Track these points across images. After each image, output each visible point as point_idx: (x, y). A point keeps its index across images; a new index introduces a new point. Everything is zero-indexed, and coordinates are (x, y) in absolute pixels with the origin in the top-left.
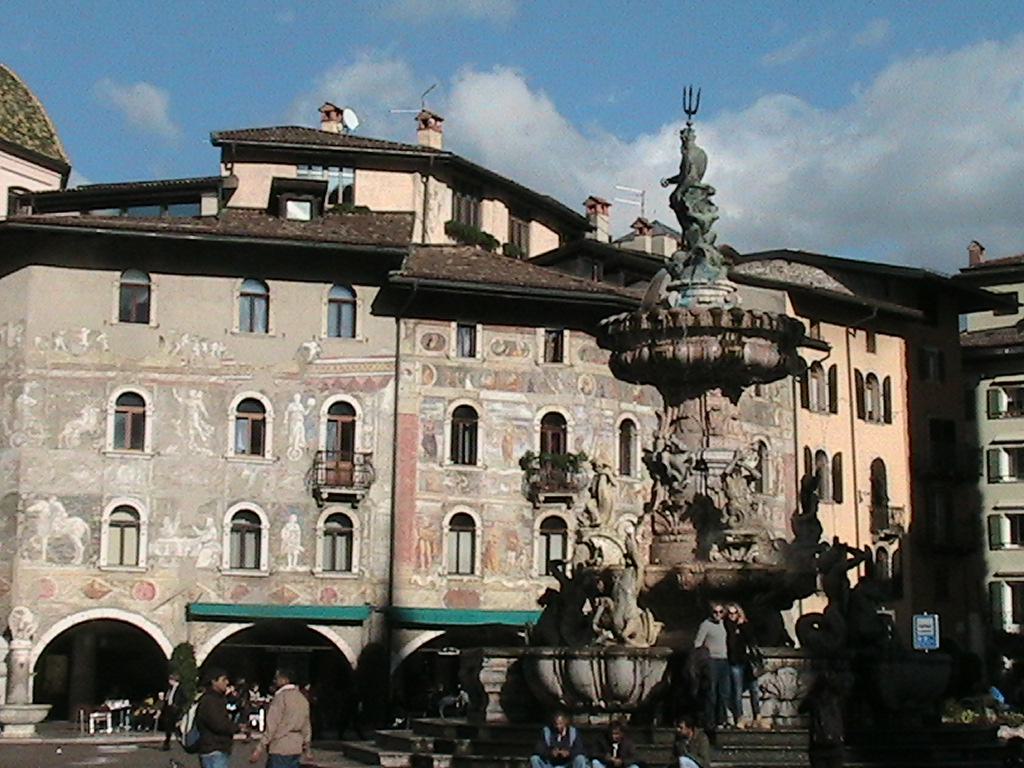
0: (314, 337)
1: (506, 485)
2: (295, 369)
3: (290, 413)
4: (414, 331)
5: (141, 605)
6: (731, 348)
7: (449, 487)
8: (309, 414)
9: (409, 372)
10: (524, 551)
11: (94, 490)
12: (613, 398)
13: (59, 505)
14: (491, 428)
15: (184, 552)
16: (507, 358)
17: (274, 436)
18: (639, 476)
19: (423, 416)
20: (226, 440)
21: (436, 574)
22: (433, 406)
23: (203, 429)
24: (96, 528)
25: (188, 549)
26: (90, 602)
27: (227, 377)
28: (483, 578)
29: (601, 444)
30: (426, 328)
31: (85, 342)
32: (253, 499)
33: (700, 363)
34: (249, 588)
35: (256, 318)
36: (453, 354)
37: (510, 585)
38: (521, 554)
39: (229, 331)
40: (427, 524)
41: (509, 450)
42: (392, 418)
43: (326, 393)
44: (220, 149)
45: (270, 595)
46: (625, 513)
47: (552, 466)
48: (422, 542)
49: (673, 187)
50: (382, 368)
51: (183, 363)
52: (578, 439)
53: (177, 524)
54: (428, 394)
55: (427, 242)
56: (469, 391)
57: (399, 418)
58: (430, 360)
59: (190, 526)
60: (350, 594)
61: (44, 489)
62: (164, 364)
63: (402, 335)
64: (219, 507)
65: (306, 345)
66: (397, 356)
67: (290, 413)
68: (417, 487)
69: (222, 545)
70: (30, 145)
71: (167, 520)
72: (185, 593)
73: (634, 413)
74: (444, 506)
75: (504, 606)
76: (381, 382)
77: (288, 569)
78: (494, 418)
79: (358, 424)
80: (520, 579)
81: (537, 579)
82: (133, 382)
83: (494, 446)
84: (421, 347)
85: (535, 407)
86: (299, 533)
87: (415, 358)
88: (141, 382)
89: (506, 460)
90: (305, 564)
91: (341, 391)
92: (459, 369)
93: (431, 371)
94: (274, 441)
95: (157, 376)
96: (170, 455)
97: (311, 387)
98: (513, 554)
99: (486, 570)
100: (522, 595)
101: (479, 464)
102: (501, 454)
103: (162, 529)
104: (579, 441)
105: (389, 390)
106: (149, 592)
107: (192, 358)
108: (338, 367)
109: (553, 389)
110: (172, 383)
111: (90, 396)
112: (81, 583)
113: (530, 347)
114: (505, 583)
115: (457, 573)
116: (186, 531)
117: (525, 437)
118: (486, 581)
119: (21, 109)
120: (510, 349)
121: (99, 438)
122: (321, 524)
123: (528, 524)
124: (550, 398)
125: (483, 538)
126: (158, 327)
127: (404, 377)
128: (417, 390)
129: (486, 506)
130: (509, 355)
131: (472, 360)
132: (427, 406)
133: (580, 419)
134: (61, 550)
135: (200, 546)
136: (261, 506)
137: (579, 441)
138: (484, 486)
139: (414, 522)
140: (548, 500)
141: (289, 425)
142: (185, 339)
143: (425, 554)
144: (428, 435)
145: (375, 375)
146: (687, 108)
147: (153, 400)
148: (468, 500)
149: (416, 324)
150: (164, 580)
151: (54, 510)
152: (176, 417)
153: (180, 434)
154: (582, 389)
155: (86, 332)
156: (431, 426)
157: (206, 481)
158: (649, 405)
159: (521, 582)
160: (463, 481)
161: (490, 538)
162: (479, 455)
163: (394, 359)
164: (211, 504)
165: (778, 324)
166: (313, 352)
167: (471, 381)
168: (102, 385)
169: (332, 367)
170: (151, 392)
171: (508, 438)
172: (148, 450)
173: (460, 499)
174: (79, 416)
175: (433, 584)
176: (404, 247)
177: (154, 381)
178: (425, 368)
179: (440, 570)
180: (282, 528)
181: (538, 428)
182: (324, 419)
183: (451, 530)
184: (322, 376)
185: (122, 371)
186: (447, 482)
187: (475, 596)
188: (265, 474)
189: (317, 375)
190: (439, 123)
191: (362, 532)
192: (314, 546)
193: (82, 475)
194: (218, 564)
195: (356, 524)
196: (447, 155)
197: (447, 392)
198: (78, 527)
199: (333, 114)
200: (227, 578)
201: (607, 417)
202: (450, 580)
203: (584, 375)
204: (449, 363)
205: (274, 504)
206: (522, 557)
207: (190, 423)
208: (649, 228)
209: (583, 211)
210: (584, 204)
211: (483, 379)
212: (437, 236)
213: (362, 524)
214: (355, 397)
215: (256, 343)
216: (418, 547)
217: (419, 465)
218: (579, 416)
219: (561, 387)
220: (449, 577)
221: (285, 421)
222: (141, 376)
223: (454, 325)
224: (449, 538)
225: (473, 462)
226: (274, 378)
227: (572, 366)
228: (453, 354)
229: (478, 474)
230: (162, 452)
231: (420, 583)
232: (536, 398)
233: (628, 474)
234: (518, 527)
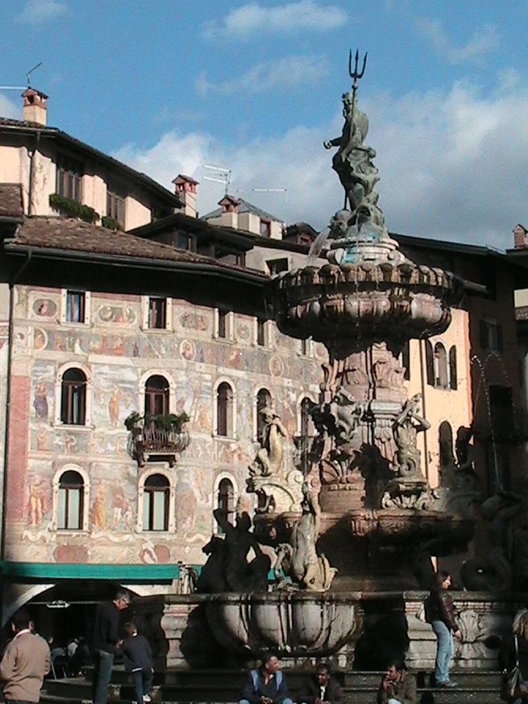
1: (112, 444)
6: (399, 304)
7: (60, 446)
10: (130, 507)
12: (212, 363)
14: (99, 389)
16: (114, 323)
18: (235, 436)
19: (35, 378)
21: (47, 530)
22: (45, 369)
28: (90, 533)
29: (201, 406)
30: (37, 294)
33: (369, 318)
36: (63, 319)
37: (116, 540)
38: (127, 510)
40: (37, 482)
41: (116, 411)
42: (6, 380)
46: (222, 471)
47: (157, 430)
48: (33, 499)
49: (336, 149)
52: (179, 401)
54: (39, 357)
55: (33, 213)
56: (77, 355)
58: (39, 324)
63: (16, 301)
68: (29, 446)
73: (230, 377)
74: (53, 463)
75: (110, 560)
78: (102, 381)
80: (126, 534)
81: (141, 534)
83: (102, 406)
85: (140, 370)
87: (29, 323)
89: (112, 420)
92: (70, 334)
93: (43, 336)
98: (120, 510)
99: (93, 525)
100: (126, 550)
101: (88, 424)
102: (108, 414)
104: (181, 402)
109: (157, 353)
113: (136, 313)
114: (112, 538)
115: (66, 528)
117: (130, 399)
118: (94, 535)
120: (116, 315)
123: (134, 481)
124: (152, 362)
125: (90, 494)
127: (17, 340)
128: (30, 354)
129: (94, 464)
130: (115, 321)
131: (80, 325)
132: (39, 368)
133: (181, 383)
137: (181, 402)
138: (93, 445)
139: (26, 481)
140: (152, 459)
143: (36, 511)
144: (40, 397)
146: (353, 72)
148: (77, 458)
149: (28, 291)
154: (184, 354)
156: (42, 388)
158: (243, 370)
159: (126, 537)
160: (72, 440)
161: (98, 495)
162: (88, 417)
163: (7, 324)
165: (443, 280)
167: (80, 345)
171: (115, 399)
173: (68, 457)
175: (43, 539)
176: (18, 216)
178: (37, 332)
179: (50, 525)
181: (143, 391)
183: (60, 487)
186: (58, 441)
187: (84, 551)
190: (44, 100)
196: (54, 131)
197: (58, 355)
201: (207, 381)
202: (60, 535)
203: (186, 341)
204: (59, 328)
206: (127, 513)
208: (236, 205)
209: (172, 189)
210: (173, 182)
211: (91, 343)
212: (43, 208)
216: (30, 504)
217: (31, 425)
218: (180, 379)
219: (163, 351)
220: (58, 533)
223: (64, 291)
224: (59, 495)
225: (81, 421)
227: (174, 332)
228: (63, 319)
229: (86, 434)
231: (31, 538)
232: (141, 362)
233: (225, 434)
234: (123, 484)
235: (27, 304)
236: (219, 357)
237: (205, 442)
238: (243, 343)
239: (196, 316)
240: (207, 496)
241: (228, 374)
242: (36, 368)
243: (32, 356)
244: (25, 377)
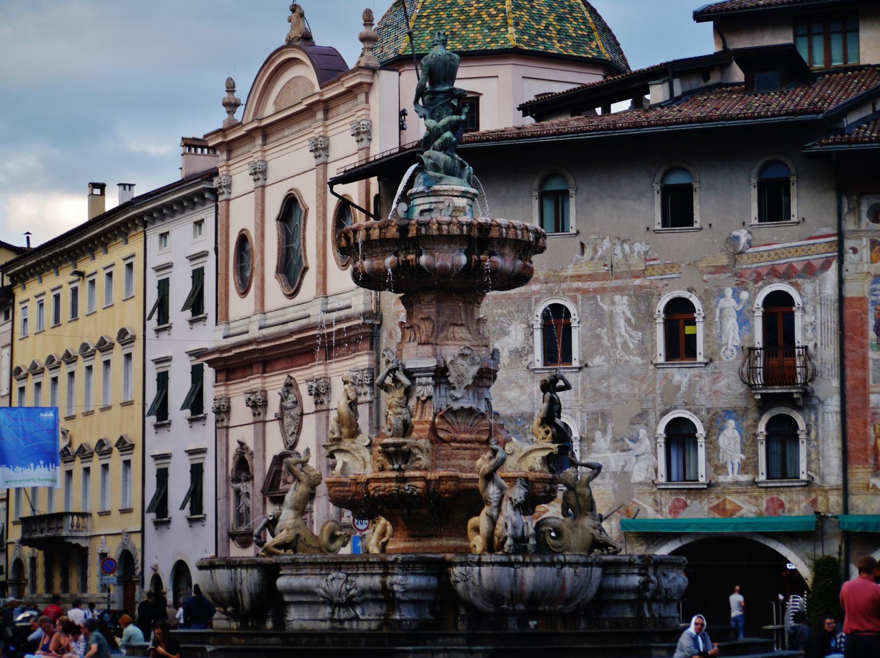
0: (744, 223)
2: (724, 260)
3: (721, 311)
4: (859, 204)
8: (743, 308)
9: (855, 250)
15: (617, 466)
17: (706, 336)
19: (874, 298)
20: (654, 346)
23: (630, 336)
25: (621, 463)
27: (652, 278)
32: (686, 406)
34: (688, 502)
35: (678, 212)
39: (651, 229)
42: (837, 305)
43: (760, 283)
44: (710, 25)
45: (711, 509)
51: (606, 268)
53: (609, 436)
57: (847, 304)
58: (876, 234)
59: (622, 440)
60: (798, 503)
62: (586, 270)
63: (846, 210)
64: (651, 417)
65: (735, 233)
66: (841, 235)
67: (721, 311)
69: (656, 458)
70: (556, 48)
71: (598, 434)
72: (622, 509)
76: (823, 264)
77: (730, 478)
79: (798, 315)
82: (557, 293)
84: (867, 220)
86: (739, 439)
90: (747, 473)
91: (776, 280)
94: (705, 342)
95: (579, 284)
96: (598, 366)
97: (743, 279)
103: (594, 444)
105: (832, 274)
107: (615, 262)
108: (772, 254)
110: (596, 291)
111: (517, 311)
116: (619, 445)
119: (552, 9)
121: (528, 354)
122: (762, 428)
126: (578, 233)
127: (849, 256)
128: (866, 269)
135: (634, 459)
136: (696, 414)
139: (869, 420)
141: (721, 323)
142: (606, 244)
145: (816, 259)
147: (578, 311)
149: (860, 196)
152: (601, 326)
153: (609, 344)
157: (636, 391)
164: (643, 415)
166: (743, 240)
169: (766, 254)
170: (576, 302)
177: (578, 290)
180: (719, 434)
184: (755, 265)
185: (546, 283)
188: (697, 379)
189: (750, 266)
191: (808, 434)
192: (756, 453)
194: (654, 477)
195: (802, 425)
200: (663, 492)
205: (708, 410)
207: (616, 330)
213: (807, 425)
214: (791, 284)
215: (679, 238)
221: (717, 319)
222: (564, 286)
226: (702, 273)
230: (589, 364)
235: (859, 212)
242: (875, 286)
243: (868, 273)
244: (862, 298)
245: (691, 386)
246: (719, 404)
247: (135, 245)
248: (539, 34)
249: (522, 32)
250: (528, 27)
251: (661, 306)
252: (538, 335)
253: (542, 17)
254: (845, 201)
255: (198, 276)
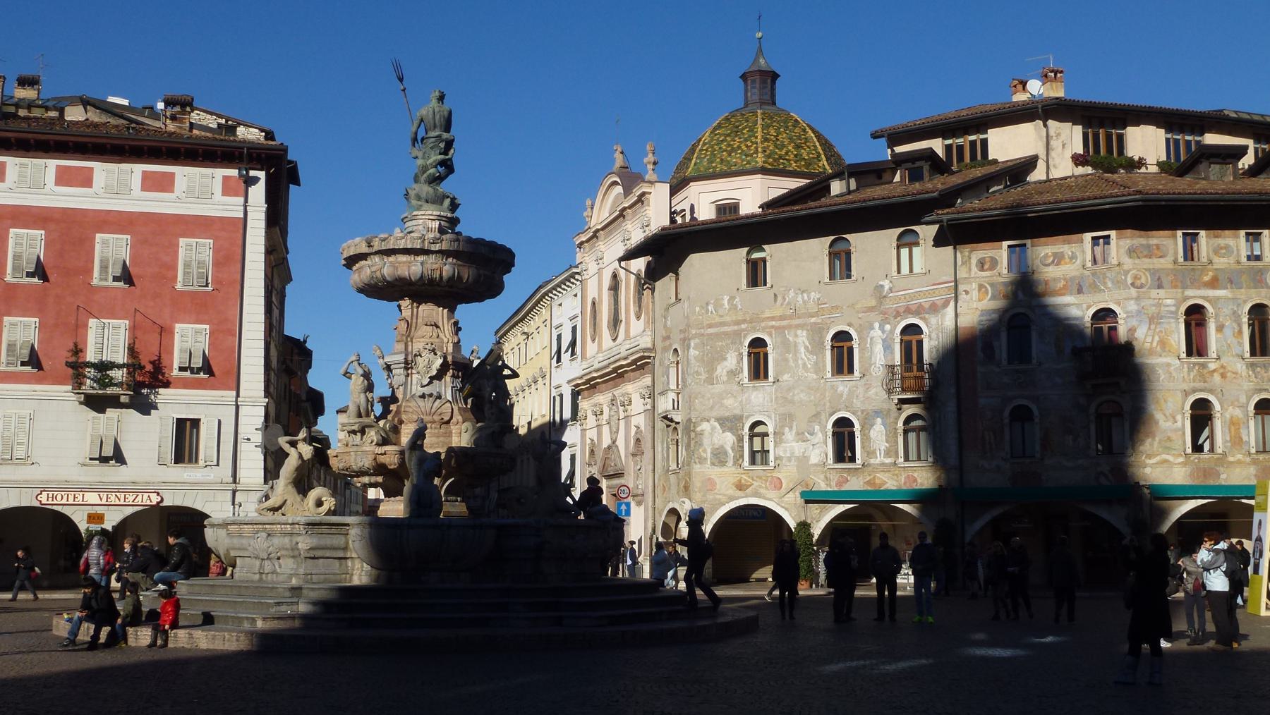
2: (873, 303)
5: (772, 494)
9: (967, 292)
11: (737, 412)
12: (1176, 287)
13: (716, 424)
20: (825, 366)
24: (740, 440)
26: (739, 493)
31: (726, 306)
32: (847, 409)
50: (945, 292)
61: (706, 414)
62: (778, 313)
64: (823, 417)
66: (956, 281)
77: (878, 461)
88: (764, 329)
101: (1034, 361)
105: (950, 310)
106: (778, 484)
110: (784, 328)
112: (733, 480)
116: (801, 437)
122: (900, 424)
124: (1098, 297)
127: (962, 296)
134: (719, 457)
142: (792, 293)
145: (938, 299)
149: (971, 252)
150: (788, 474)
151: (713, 428)
152: (788, 352)
154: (1132, 284)
155: (726, 298)
164: (817, 415)
166: (887, 288)
168: (738, 335)
172: (771, 379)
174: (725, 359)
177: (773, 327)
178: (981, 287)
182: (898, 340)
193: (729, 402)
198: (728, 439)
199: (1020, 87)
205: (863, 411)
215: (841, 286)
218: (1130, 308)
219: (1110, 285)
233: (1200, 354)
236: (1183, 279)
237: (1169, 365)
238: (1221, 263)
239: (1149, 246)
240: (1174, 418)
241: (1196, 296)
245: (851, 393)
246: (870, 407)
247: (545, 312)
248: (781, 157)
249: (769, 156)
250: (773, 153)
251: (829, 337)
252: (745, 359)
253: (783, 146)
254: (959, 255)
255: (574, 329)
